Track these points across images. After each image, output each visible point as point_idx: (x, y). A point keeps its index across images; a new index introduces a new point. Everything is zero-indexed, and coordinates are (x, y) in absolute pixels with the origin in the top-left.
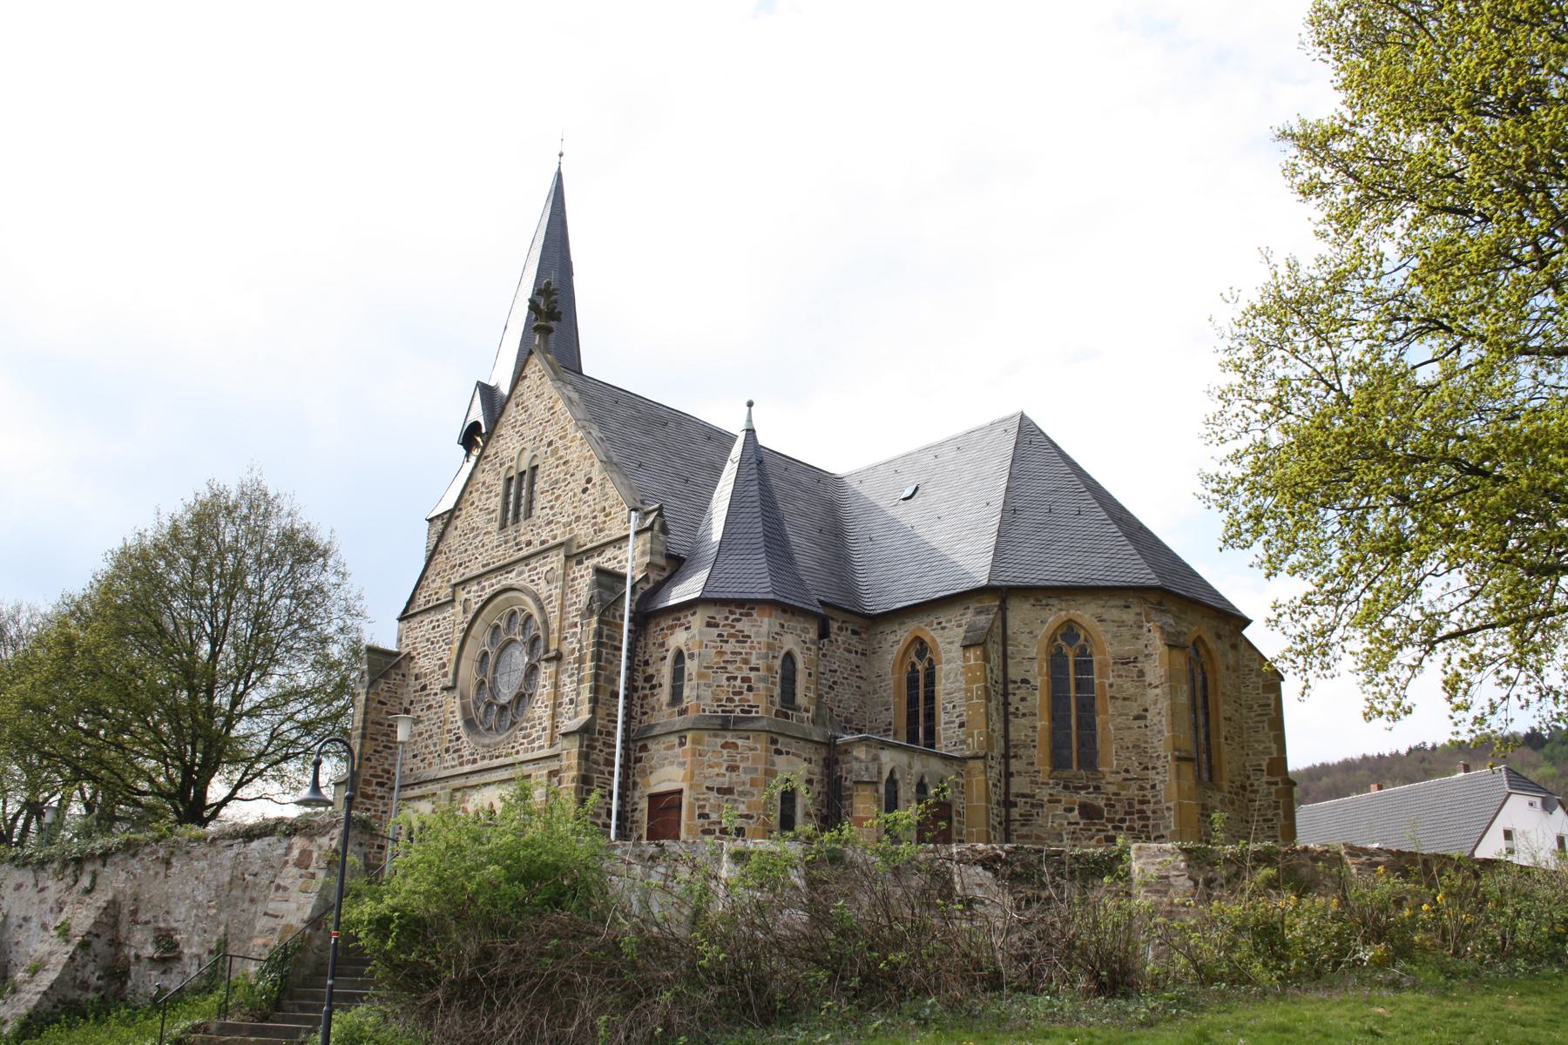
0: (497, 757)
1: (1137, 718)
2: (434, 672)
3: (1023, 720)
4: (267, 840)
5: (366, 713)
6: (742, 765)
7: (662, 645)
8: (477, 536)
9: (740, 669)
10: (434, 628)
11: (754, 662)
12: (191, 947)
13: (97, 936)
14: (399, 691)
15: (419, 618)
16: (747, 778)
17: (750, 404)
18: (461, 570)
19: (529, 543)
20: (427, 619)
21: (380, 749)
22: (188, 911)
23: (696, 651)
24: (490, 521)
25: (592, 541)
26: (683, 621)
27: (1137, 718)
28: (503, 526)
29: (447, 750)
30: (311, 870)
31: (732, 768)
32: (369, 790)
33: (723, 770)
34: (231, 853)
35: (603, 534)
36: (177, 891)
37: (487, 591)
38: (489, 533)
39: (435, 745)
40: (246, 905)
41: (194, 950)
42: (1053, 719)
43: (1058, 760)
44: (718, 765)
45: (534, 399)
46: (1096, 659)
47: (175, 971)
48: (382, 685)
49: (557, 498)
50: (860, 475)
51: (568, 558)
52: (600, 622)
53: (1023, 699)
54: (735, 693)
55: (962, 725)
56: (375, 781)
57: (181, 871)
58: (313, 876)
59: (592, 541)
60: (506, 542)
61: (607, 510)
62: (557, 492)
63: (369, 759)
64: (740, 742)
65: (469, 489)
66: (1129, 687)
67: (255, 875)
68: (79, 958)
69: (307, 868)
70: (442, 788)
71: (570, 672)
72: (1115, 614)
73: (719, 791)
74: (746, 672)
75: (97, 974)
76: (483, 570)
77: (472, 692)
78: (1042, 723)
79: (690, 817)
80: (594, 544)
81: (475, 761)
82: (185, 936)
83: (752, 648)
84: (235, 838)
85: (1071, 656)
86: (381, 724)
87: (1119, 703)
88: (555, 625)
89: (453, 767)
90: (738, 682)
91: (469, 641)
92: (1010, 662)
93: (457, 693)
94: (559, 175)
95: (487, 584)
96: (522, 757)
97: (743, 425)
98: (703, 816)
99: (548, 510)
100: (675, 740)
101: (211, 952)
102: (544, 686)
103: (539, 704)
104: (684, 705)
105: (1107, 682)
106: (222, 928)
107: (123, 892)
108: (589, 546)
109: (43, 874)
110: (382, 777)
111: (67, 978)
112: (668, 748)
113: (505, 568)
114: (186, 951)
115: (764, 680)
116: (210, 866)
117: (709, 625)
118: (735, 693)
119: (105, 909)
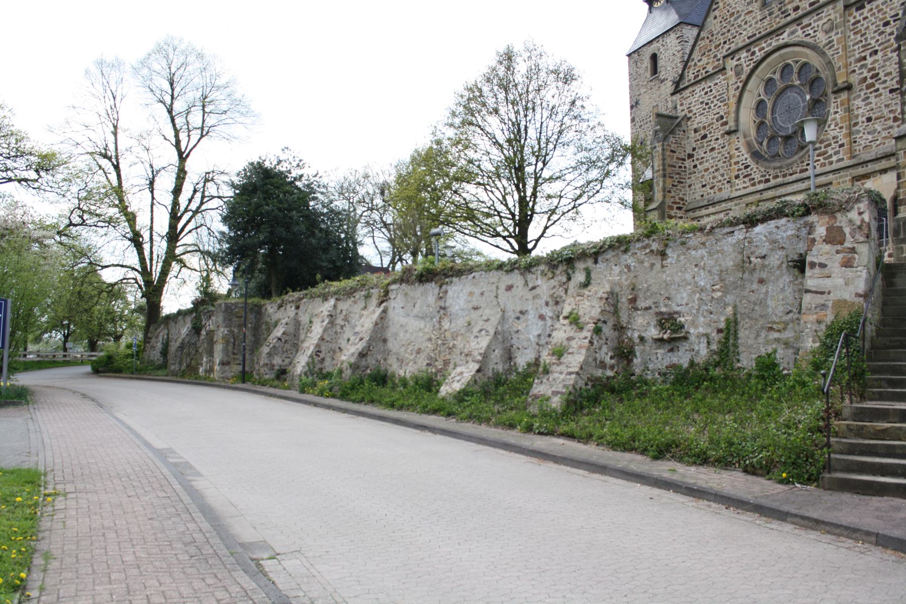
0: (791, 175)
2: (712, 123)
4: (772, 224)
5: (664, 159)
8: (739, 16)
10: (706, 93)
12: (696, 327)
13: (605, 322)
14: (683, 143)
15: (691, 89)
18: (727, 46)
19: (796, 9)
20: (697, 88)
21: (676, 183)
22: (690, 295)
29: (737, 177)
32: (672, 213)
34: (731, 240)
36: (677, 279)
37: (758, 54)
38: (751, 12)
39: (722, 175)
40: (755, 286)
41: (701, 330)
47: (682, 349)
48: (671, 139)
56: (675, 206)
57: (678, 261)
58: (853, 250)
60: (770, 14)
63: (670, 192)
67: (764, 257)
68: (595, 342)
69: (842, 244)
70: (736, 205)
71: (863, 96)
75: (610, 354)
76: (748, 41)
77: (753, 133)
81: (767, 181)
82: (689, 318)
84: (737, 224)
86: (674, 167)
88: (838, 63)
89: (744, 188)
91: (746, 95)
93: (740, 135)
95: (756, 49)
101: (720, 331)
102: (836, 113)
103: (832, 127)
106: (729, 310)
107: (619, 284)
109: (529, 276)
110: (679, 203)
111: (591, 359)
114: (692, 331)
116: (710, 254)
119: (607, 299)
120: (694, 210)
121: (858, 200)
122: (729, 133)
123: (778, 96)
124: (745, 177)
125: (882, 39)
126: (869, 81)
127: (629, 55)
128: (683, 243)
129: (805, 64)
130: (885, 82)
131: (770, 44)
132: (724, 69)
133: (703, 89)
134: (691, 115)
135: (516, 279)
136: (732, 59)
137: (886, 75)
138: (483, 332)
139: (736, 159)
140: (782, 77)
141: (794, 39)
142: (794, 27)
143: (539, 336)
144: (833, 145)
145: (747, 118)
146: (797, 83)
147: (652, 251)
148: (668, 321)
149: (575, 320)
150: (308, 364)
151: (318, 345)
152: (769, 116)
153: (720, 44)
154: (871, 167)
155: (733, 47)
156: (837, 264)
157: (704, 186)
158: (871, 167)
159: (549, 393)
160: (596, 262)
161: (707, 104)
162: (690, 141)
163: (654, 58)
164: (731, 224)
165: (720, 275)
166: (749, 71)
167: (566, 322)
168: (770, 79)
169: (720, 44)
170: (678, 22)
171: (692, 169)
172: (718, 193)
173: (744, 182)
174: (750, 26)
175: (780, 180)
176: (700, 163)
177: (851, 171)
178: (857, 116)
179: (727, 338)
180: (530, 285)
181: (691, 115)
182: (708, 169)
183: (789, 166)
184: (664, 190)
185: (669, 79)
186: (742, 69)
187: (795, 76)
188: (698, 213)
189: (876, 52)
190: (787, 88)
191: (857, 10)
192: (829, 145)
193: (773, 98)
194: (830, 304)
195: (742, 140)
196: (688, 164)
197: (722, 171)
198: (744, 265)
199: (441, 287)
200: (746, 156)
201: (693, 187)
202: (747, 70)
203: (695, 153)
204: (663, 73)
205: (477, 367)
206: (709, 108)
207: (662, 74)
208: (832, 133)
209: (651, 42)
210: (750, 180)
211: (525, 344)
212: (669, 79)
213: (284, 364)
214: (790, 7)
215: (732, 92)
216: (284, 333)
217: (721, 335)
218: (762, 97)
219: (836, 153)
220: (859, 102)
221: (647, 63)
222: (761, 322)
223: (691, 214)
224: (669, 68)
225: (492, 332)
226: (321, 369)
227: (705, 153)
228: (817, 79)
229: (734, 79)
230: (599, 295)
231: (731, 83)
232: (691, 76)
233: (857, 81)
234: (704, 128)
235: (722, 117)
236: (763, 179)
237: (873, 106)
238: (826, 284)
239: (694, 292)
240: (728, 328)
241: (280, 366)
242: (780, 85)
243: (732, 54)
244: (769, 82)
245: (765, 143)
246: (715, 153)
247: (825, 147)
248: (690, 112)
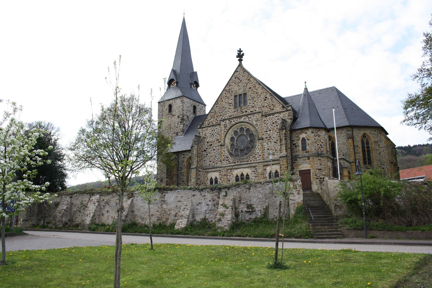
0: (243, 162)
1: (379, 154)
3: (358, 154)
6: (323, 164)
7: (298, 137)
8: (226, 109)
9: (319, 143)
11: (322, 141)
12: (258, 208)
15: (206, 128)
16: (324, 167)
17: (305, 82)
19: (246, 112)
20: (209, 129)
22: (256, 200)
23: (310, 139)
24: (229, 106)
25: (269, 112)
26: (304, 131)
27: (379, 154)
28: (235, 107)
30: (298, 189)
31: (321, 165)
33: (319, 165)
35: (273, 111)
36: (253, 195)
37: (232, 122)
38: (230, 108)
39: (218, 159)
40: (274, 198)
42: (363, 154)
43: (365, 163)
44: (318, 164)
45: (241, 77)
46: (370, 141)
47: (253, 214)
49: (255, 101)
50: (287, 98)
51: (262, 116)
52: (286, 131)
53: (357, 150)
54: (319, 148)
55: (343, 155)
57: (254, 191)
58: (299, 191)
59: (269, 112)
60: (237, 111)
61: (274, 105)
62: (255, 100)
64: (322, 159)
65: (220, 98)
66: (377, 148)
70: (223, 169)
71: (266, 142)
72: (373, 132)
73: (319, 170)
74: (321, 144)
77: (229, 147)
78: (361, 155)
79: (313, 175)
80: (271, 113)
83: (321, 138)
84: (270, 182)
85: (365, 140)
87: (375, 151)
90: (319, 146)
92: (354, 142)
94: (184, 19)
95: (232, 121)
96: (252, 162)
97: (304, 87)
98: (316, 175)
99: (252, 104)
100: (307, 158)
101: (264, 209)
102: (258, 145)
103: (257, 149)
104: (307, 151)
105: (373, 147)
106: (267, 204)
107: (236, 196)
108: (269, 113)
109: (202, 192)
112: (304, 160)
113: (240, 117)
114: (256, 209)
115: (324, 145)
116: (262, 189)
117: (312, 133)
118: (319, 148)
120: (206, 169)
121: (298, 179)
122: (221, 145)
123: (238, 137)
124: (226, 160)
125: (272, 127)
126: (268, 138)
127: (159, 103)
128: (255, 186)
129: (248, 129)
130: (273, 139)
131: (237, 120)
132: (220, 124)
133: (211, 129)
134: (206, 137)
135: (197, 193)
136: (223, 122)
137: (273, 137)
138: (186, 209)
139: (224, 154)
140: (240, 131)
141: (245, 121)
142: (245, 117)
143: (206, 210)
144: (257, 155)
145: (228, 141)
146: (245, 134)
147: (246, 188)
148: (250, 206)
149: (225, 206)
150: (91, 220)
151: (94, 213)
152: (235, 142)
153: (218, 116)
154: (269, 163)
155: (223, 118)
156: (296, 194)
157: (210, 161)
158: (269, 163)
159: (223, 226)
160: (229, 190)
161: (212, 134)
162: (206, 146)
163: (170, 106)
164: (269, 182)
165: (265, 195)
166: (229, 127)
167: (222, 206)
168: (236, 131)
169: (218, 116)
170: (182, 95)
171: (206, 155)
172: (216, 164)
173: (226, 162)
174: (230, 113)
175: (239, 163)
176: (209, 154)
177: (263, 163)
178: (265, 148)
179: (266, 211)
180: (203, 195)
181: (206, 137)
182: (212, 156)
183: (242, 159)
184: (197, 161)
185: (177, 115)
186: (227, 126)
187: (245, 132)
188: (208, 170)
189: (270, 130)
190: (242, 135)
191: (265, 117)
192: (256, 155)
193: (237, 137)
194: (296, 203)
195: (226, 149)
196: (204, 153)
197: (217, 157)
198: (272, 193)
199: (162, 194)
200: (227, 154)
201: (206, 161)
202: (229, 127)
203: (207, 150)
204: (174, 112)
205: (187, 220)
206: (213, 136)
207: (173, 113)
208: (257, 151)
209: (169, 100)
210: (229, 162)
211: (200, 213)
212: (177, 115)
213: (66, 220)
214: (244, 110)
215: (223, 133)
216: (67, 208)
217: (264, 210)
218: (233, 136)
219: (258, 157)
220: (265, 144)
221: (167, 107)
222: (275, 207)
223: (205, 170)
224: (176, 111)
225: (189, 209)
226: (95, 222)
227: (211, 150)
228: (252, 134)
229: (224, 128)
230: (231, 199)
231: (222, 129)
232: (207, 124)
233: (265, 138)
234: (211, 142)
235: (218, 140)
236: (233, 162)
237: (269, 145)
238: (294, 198)
239: (258, 199)
240: (266, 208)
241: (65, 221)
242: (240, 134)
243: (224, 120)
244: (236, 132)
245: (233, 151)
246: (215, 151)
247: (255, 155)
248: (205, 136)
